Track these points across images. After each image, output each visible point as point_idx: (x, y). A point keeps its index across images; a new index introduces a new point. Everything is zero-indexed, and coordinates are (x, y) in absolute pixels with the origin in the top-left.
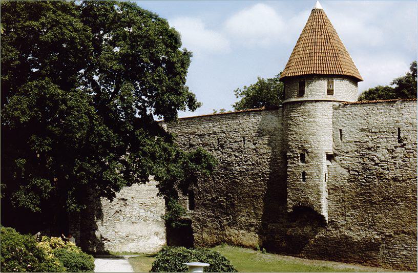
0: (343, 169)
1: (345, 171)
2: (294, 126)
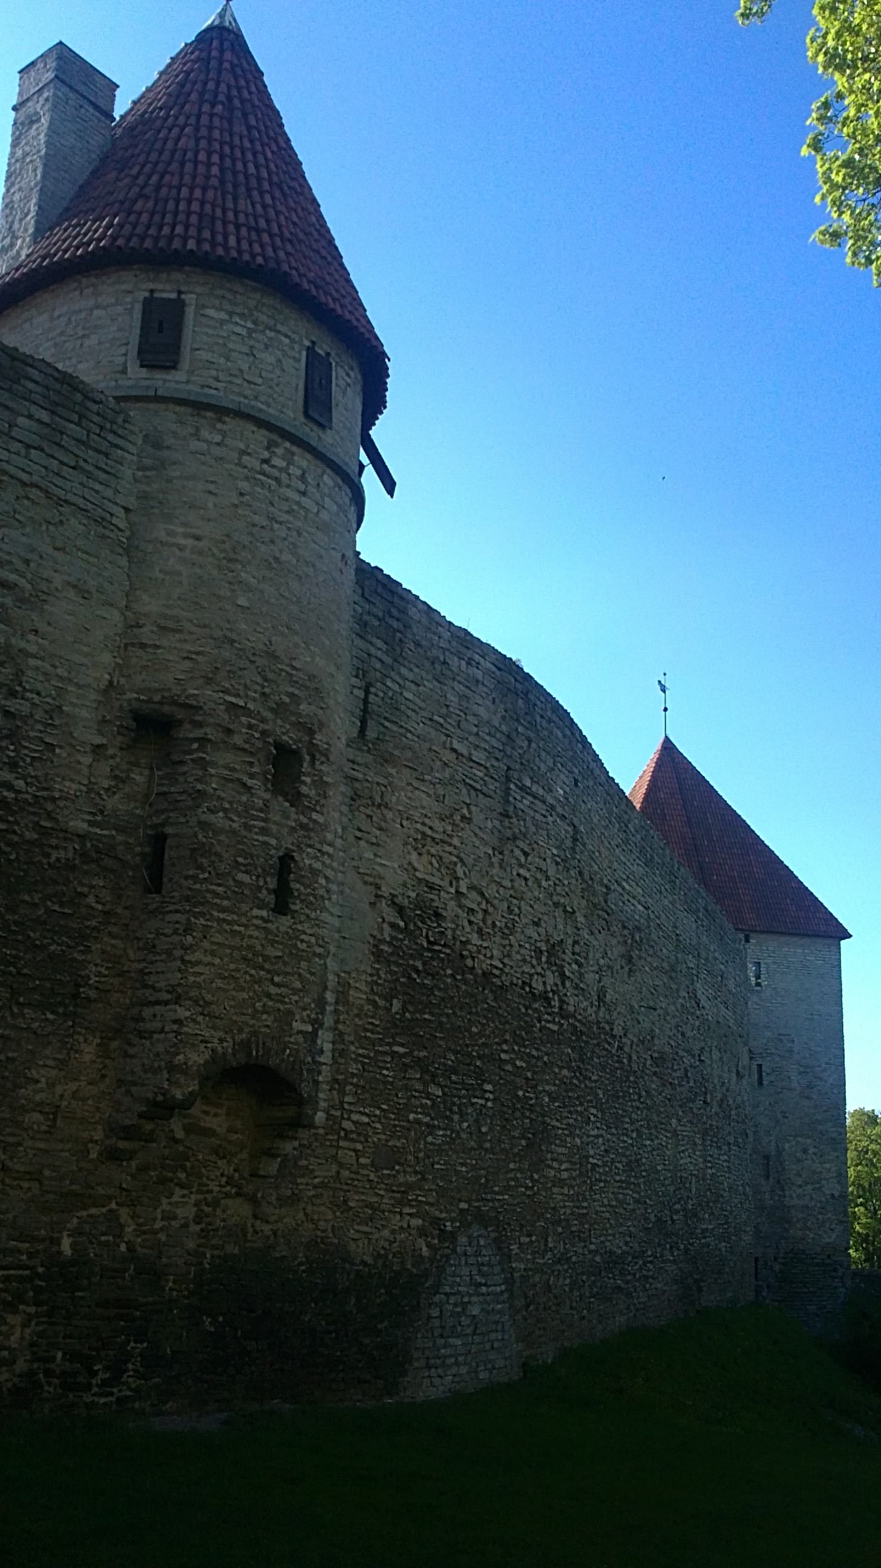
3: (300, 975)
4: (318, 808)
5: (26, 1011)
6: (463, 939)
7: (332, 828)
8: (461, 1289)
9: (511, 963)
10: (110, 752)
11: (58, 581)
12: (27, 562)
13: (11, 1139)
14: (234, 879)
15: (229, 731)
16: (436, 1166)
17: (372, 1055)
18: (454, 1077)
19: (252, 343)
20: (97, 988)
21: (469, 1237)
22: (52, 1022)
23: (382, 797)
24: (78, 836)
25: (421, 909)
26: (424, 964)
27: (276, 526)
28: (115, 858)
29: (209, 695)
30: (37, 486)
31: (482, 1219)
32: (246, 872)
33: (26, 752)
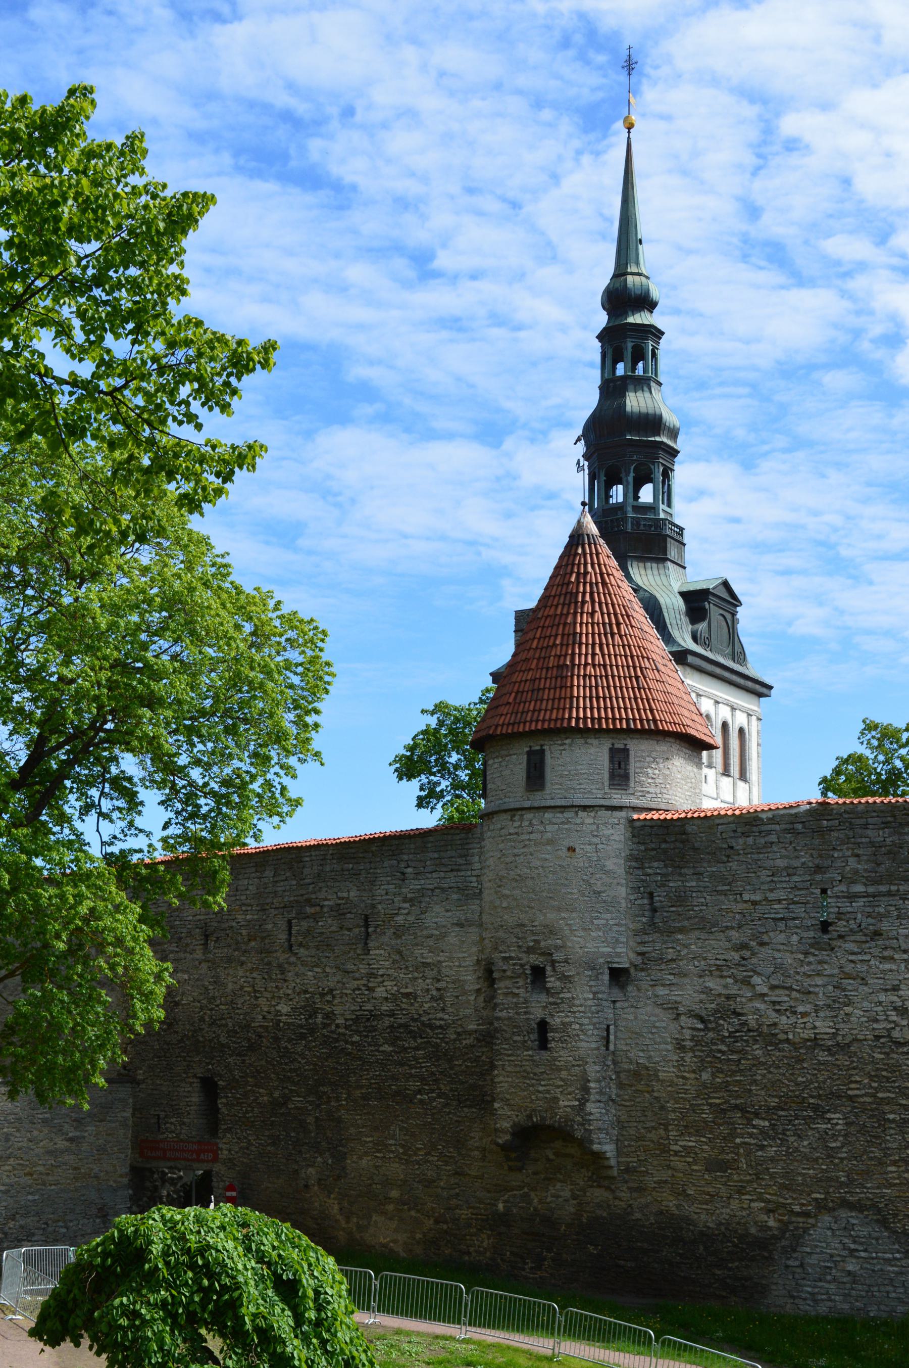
0: (658, 1011)
1: (664, 1019)
2: (515, 884)
15: (504, 971)
26: (728, 1046)
27: (517, 858)
32: (519, 1035)
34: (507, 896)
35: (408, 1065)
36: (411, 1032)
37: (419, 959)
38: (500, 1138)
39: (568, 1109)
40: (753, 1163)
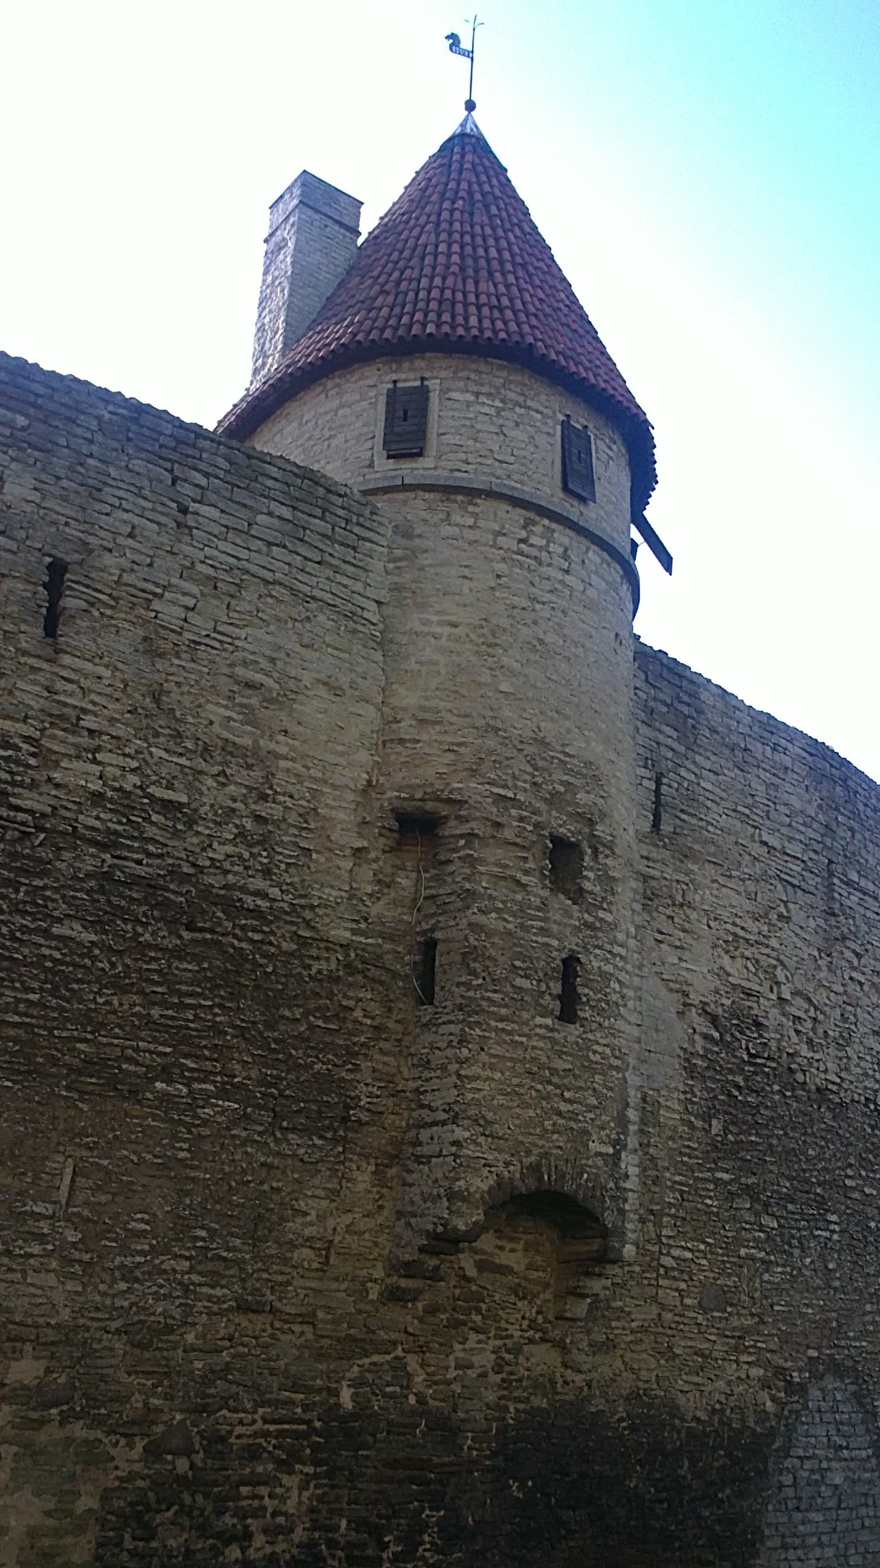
3: (594, 1090)
4: (605, 906)
5: (290, 1136)
6: (791, 1051)
7: (624, 927)
8: (817, 1452)
9: (851, 1078)
10: (373, 855)
11: (307, 678)
12: (273, 660)
13: (280, 1278)
14: (513, 986)
15: (498, 825)
16: (776, 1308)
17: (691, 1182)
18: (790, 1207)
19: (501, 421)
20: (369, 1110)
21: (822, 1390)
22: (320, 1148)
23: (683, 897)
24: (341, 946)
25: (739, 1019)
26: (746, 1079)
27: (538, 607)
28: (384, 968)
29: (472, 788)
30: (281, 584)
31: (837, 1369)
32: (526, 977)
33: (280, 857)
34: (513, 674)
35: (141, 992)
36: (165, 904)
37: (216, 728)
38: (461, 1215)
39: (600, 1162)
40: (757, 1295)
